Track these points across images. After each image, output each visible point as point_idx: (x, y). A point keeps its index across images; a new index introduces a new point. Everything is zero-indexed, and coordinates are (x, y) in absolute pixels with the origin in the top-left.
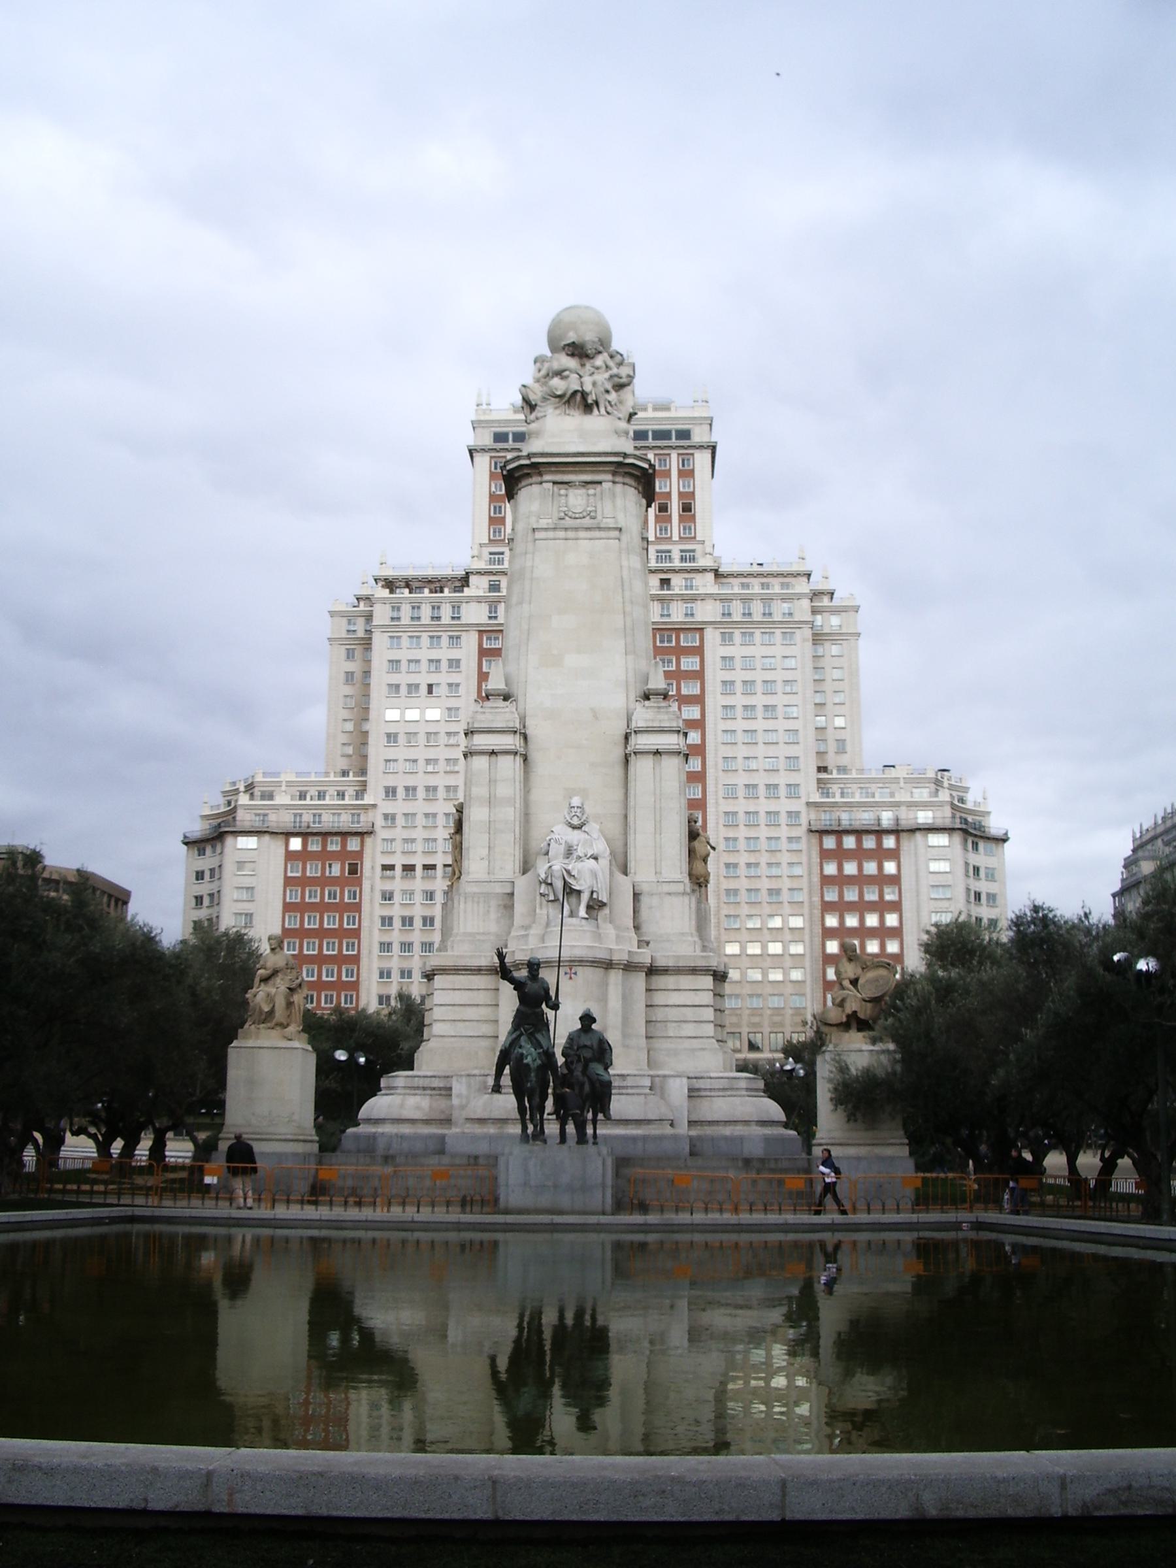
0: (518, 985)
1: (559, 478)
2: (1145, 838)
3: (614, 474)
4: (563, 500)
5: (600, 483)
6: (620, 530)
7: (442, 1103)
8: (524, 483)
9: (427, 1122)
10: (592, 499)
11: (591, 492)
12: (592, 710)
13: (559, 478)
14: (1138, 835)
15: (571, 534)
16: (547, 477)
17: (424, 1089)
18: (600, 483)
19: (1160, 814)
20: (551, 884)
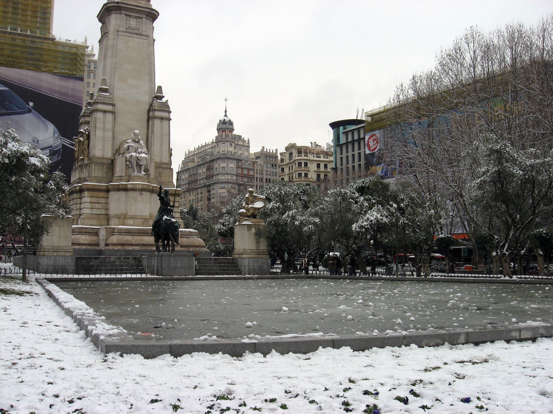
0: (161, 199)
1: (127, 13)
2: (190, 155)
3: (147, 15)
4: (128, 22)
5: (142, 18)
6: (147, 36)
7: (94, 238)
8: (113, 12)
9: (89, 245)
10: (138, 23)
11: (138, 20)
12: (137, 100)
13: (127, 13)
14: (187, 153)
15: (131, 35)
16: (123, 12)
17: (86, 232)
18: (142, 18)
19: (197, 147)
20: (131, 162)
